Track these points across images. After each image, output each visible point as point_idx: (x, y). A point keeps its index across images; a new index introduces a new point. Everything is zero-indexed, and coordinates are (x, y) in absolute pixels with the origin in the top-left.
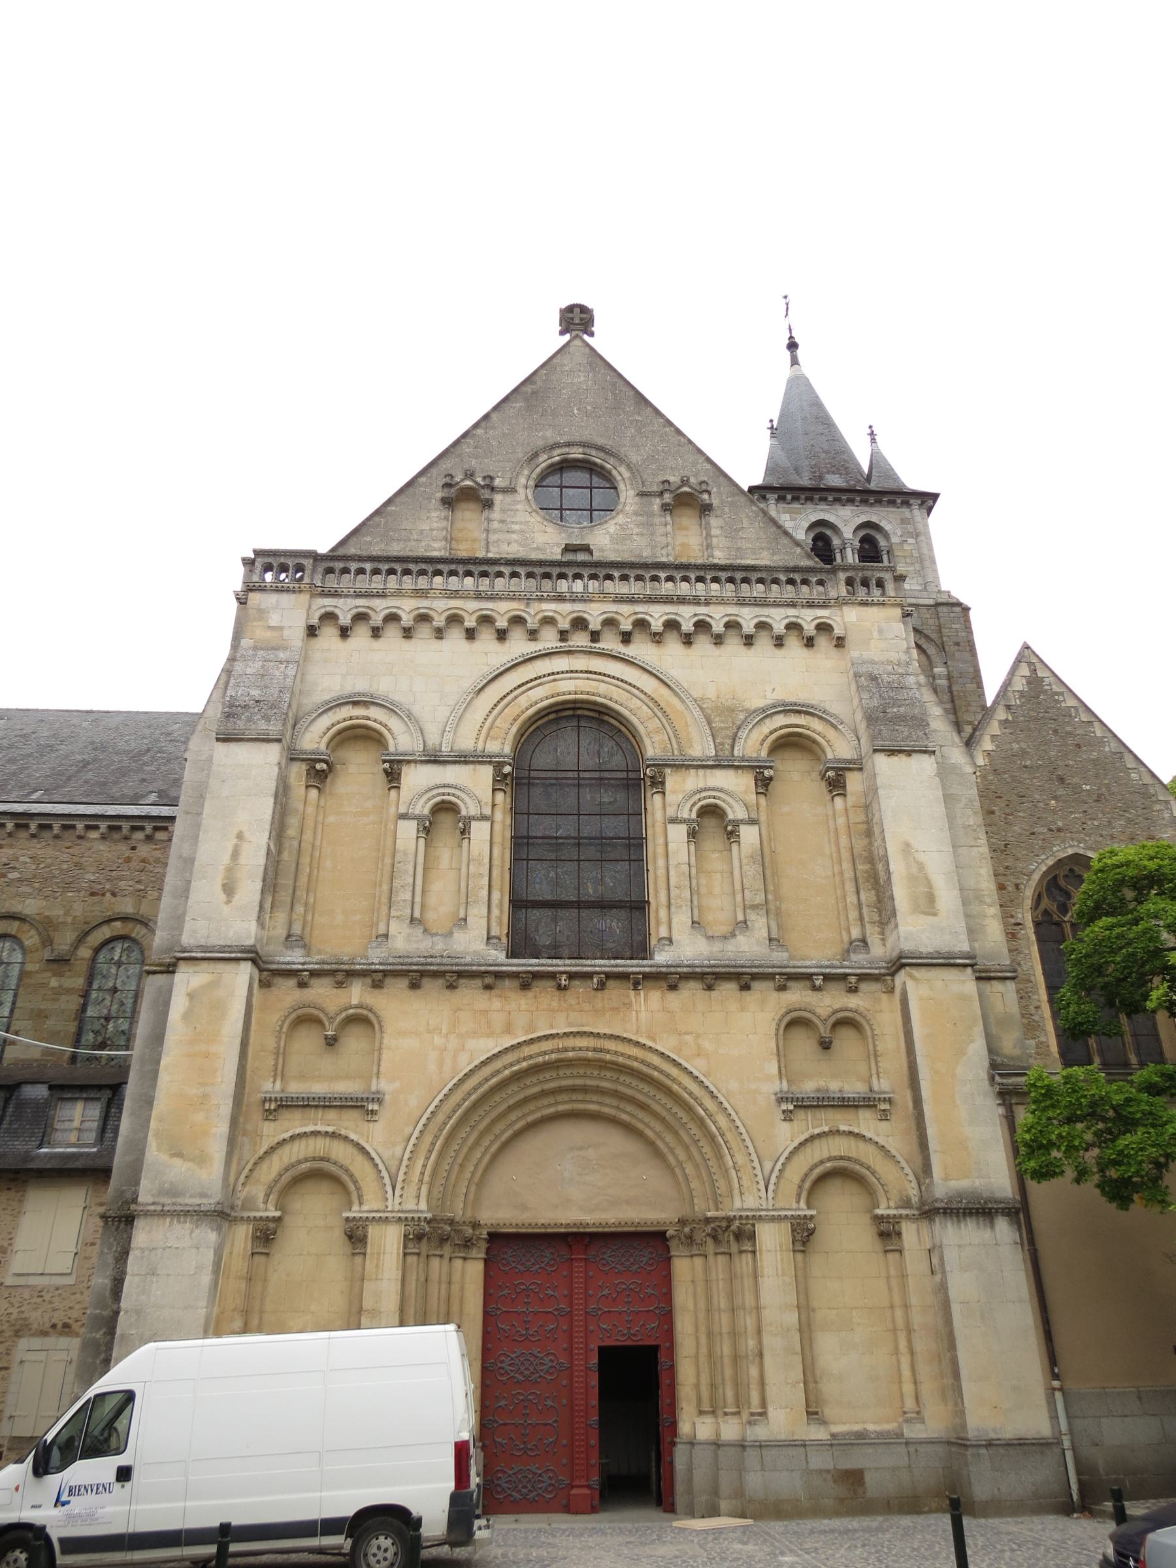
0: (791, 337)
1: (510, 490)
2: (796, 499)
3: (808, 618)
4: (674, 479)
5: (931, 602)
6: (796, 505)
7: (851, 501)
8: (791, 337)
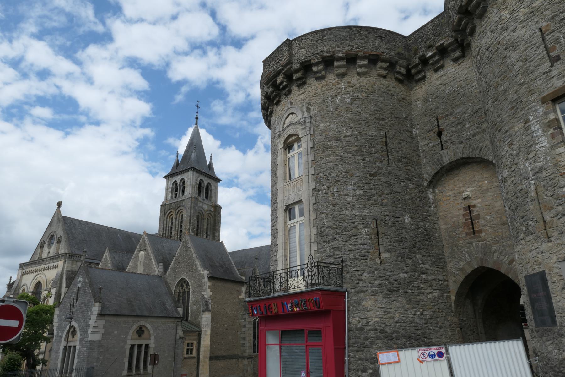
0: (197, 116)
1: (46, 243)
2: (171, 177)
3: (56, 263)
4: (59, 236)
5: (186, 198)
6: (172, 178)
7: (179, 174)
8: (197, 116)
